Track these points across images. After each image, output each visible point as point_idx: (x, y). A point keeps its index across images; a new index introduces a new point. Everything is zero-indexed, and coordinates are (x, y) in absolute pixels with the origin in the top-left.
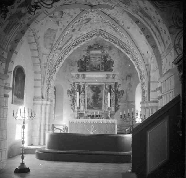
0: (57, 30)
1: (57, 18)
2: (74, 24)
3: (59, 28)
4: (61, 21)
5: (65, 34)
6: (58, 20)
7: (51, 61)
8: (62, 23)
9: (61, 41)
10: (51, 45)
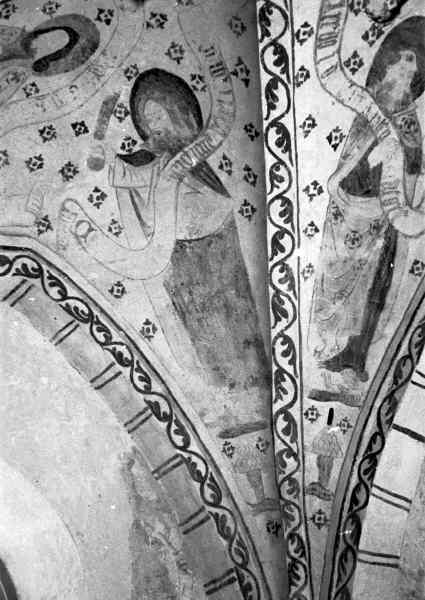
0: (232, 225)
1: (181, 148)
2: (271, 107)
3: (234, 204)
4: (219, 153)
5: (280, 221)
6: (194, 161)
7: (291, 462)
8: (226, 163)
9: (283, 288)
10: (252, 352)
